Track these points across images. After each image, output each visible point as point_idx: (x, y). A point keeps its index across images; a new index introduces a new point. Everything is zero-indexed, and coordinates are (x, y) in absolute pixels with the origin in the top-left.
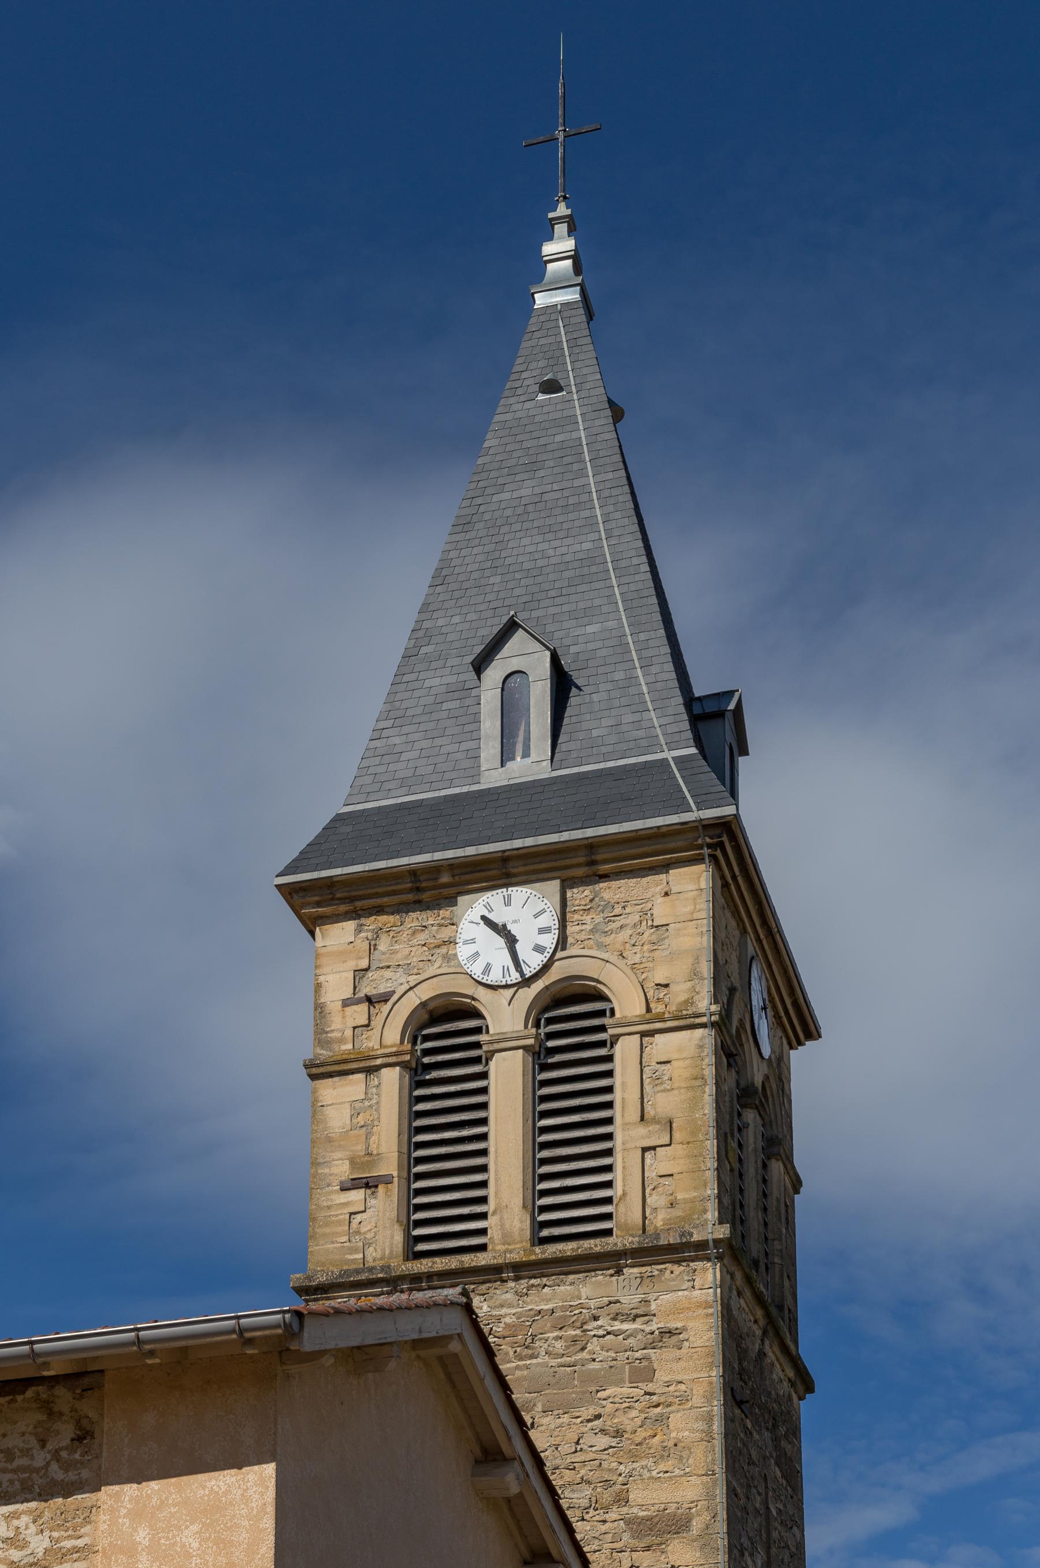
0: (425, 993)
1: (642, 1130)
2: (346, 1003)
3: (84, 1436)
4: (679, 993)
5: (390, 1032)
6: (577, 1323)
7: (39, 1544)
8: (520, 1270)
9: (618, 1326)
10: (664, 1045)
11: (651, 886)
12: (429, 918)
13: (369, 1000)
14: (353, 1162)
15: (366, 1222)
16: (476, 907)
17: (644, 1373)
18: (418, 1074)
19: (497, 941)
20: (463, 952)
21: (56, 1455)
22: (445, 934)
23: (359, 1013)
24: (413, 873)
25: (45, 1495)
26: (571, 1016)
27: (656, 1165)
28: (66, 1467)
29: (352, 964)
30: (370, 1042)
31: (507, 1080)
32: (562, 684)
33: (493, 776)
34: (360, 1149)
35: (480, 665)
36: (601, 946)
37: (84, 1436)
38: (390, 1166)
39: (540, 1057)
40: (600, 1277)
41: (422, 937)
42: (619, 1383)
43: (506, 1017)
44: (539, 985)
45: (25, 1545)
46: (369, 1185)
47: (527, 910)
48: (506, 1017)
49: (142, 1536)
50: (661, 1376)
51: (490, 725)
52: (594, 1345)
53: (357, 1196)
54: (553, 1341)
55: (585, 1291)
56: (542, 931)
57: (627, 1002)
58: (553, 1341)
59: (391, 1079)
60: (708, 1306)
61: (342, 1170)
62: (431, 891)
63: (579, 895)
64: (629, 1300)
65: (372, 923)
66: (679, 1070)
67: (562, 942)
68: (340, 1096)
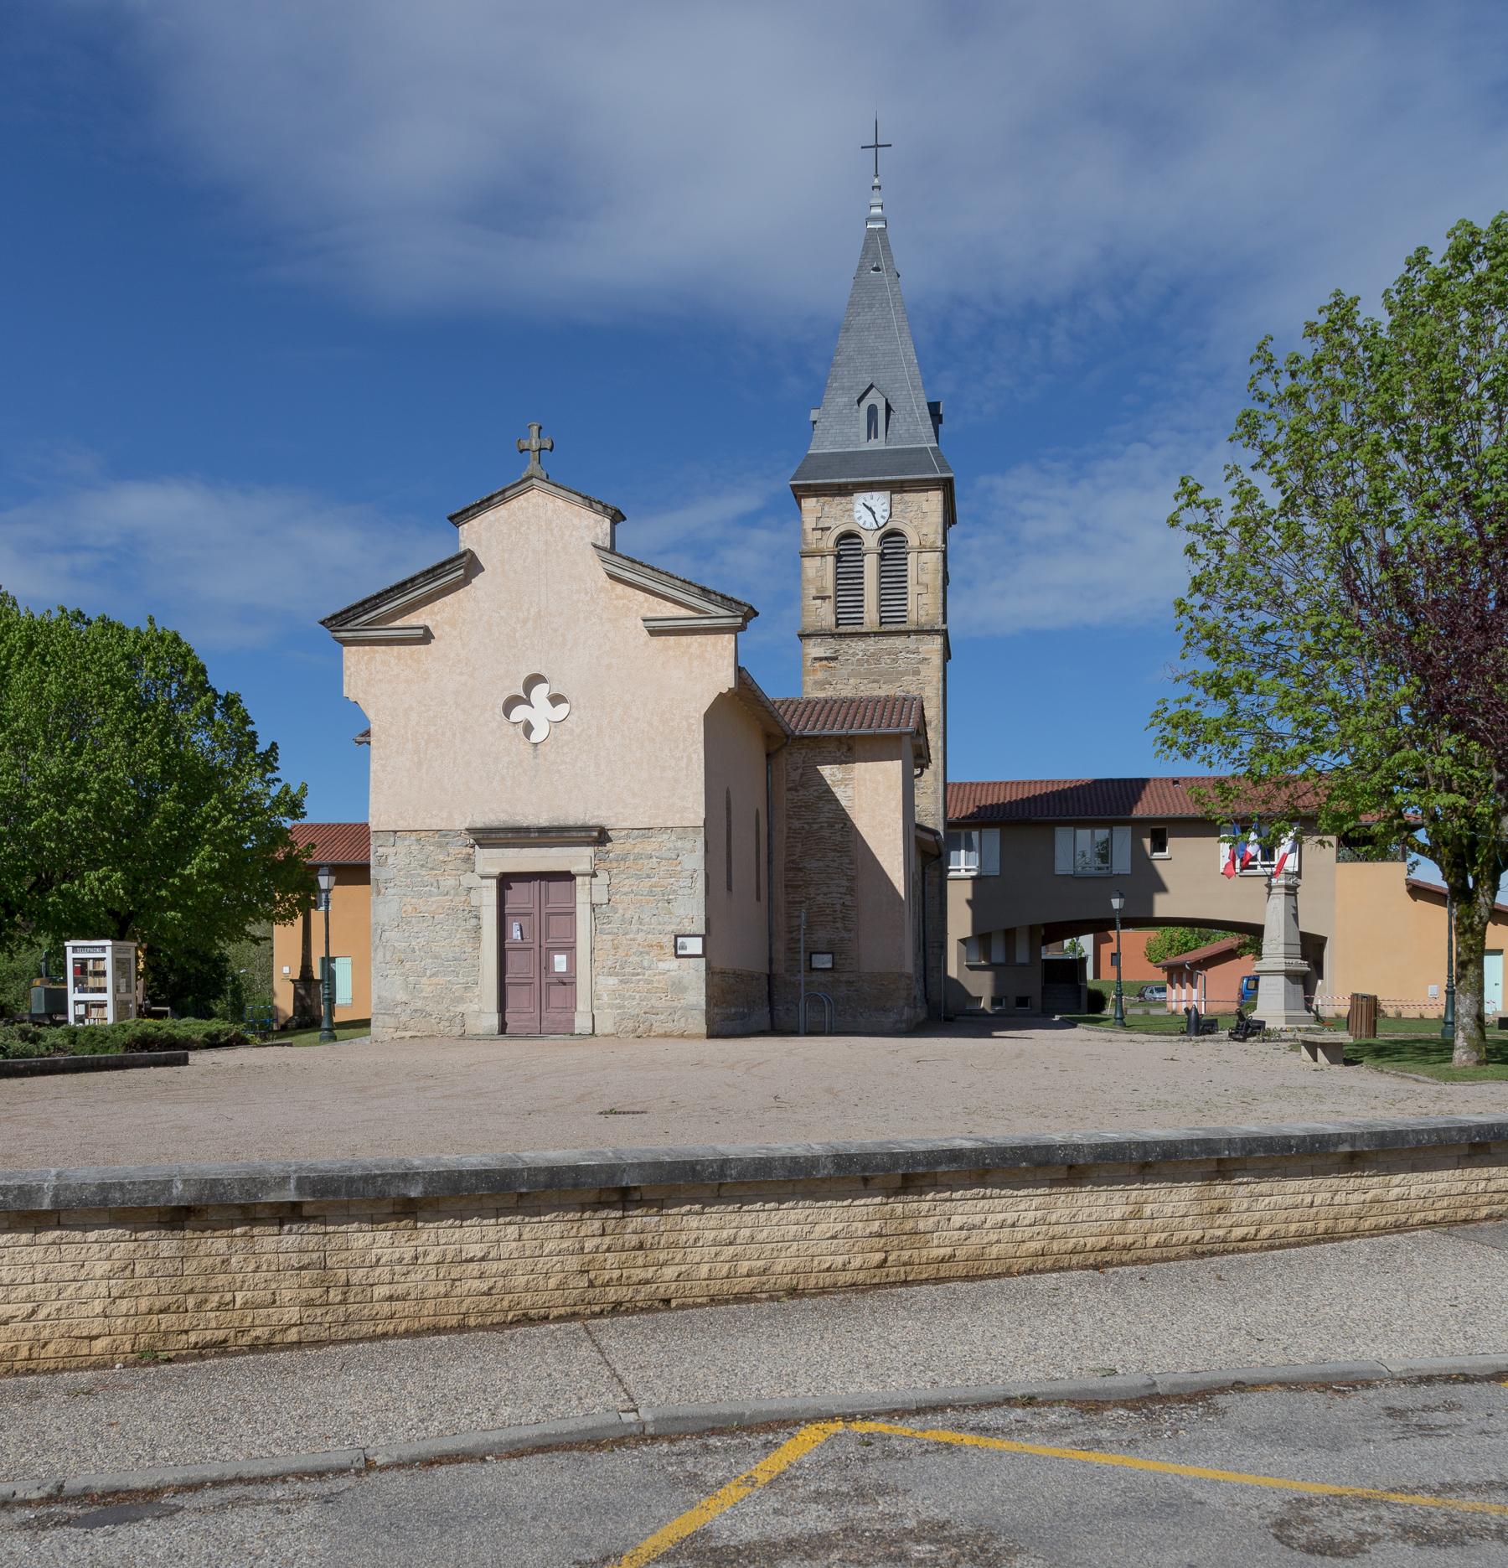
0: (842, 529)
3: (850, 749)
4: (931, 538)
5: (829, 542)
6: (894, 654)
7: (840, 776)
8: (876, 634)
10: (926, 557)
11: (922, 496)
12: (843, 500)
15: (822, 612)
16: (860, 498)
17: (917, 672)
18: (838, 558)
19: (868, 512)
20: (857, 515)
24: (839, 485)
25: (841, 763)
26: (892, 537)
27: (924, 599)
30: (822, 545)
31: (871, 564)
32: (888, 409)
33: (866, 447)
35: (859, 401)
37: (850, 749)
38: (830, 592)
39: (882, 556)
43: (871, 541)
46: (823, 598)
47: (879, 501)
48: (871, 541)
51: (864, 424)
54: (887, 659)
57: (913, 540)
58: (887, 659)
59: (830, 560)
61: (814, 593)
62: (845, 490)
63: (896, 497)
64: (912, 647)
65: (822, 499)
66: (930, 567)
68: (811, 565)
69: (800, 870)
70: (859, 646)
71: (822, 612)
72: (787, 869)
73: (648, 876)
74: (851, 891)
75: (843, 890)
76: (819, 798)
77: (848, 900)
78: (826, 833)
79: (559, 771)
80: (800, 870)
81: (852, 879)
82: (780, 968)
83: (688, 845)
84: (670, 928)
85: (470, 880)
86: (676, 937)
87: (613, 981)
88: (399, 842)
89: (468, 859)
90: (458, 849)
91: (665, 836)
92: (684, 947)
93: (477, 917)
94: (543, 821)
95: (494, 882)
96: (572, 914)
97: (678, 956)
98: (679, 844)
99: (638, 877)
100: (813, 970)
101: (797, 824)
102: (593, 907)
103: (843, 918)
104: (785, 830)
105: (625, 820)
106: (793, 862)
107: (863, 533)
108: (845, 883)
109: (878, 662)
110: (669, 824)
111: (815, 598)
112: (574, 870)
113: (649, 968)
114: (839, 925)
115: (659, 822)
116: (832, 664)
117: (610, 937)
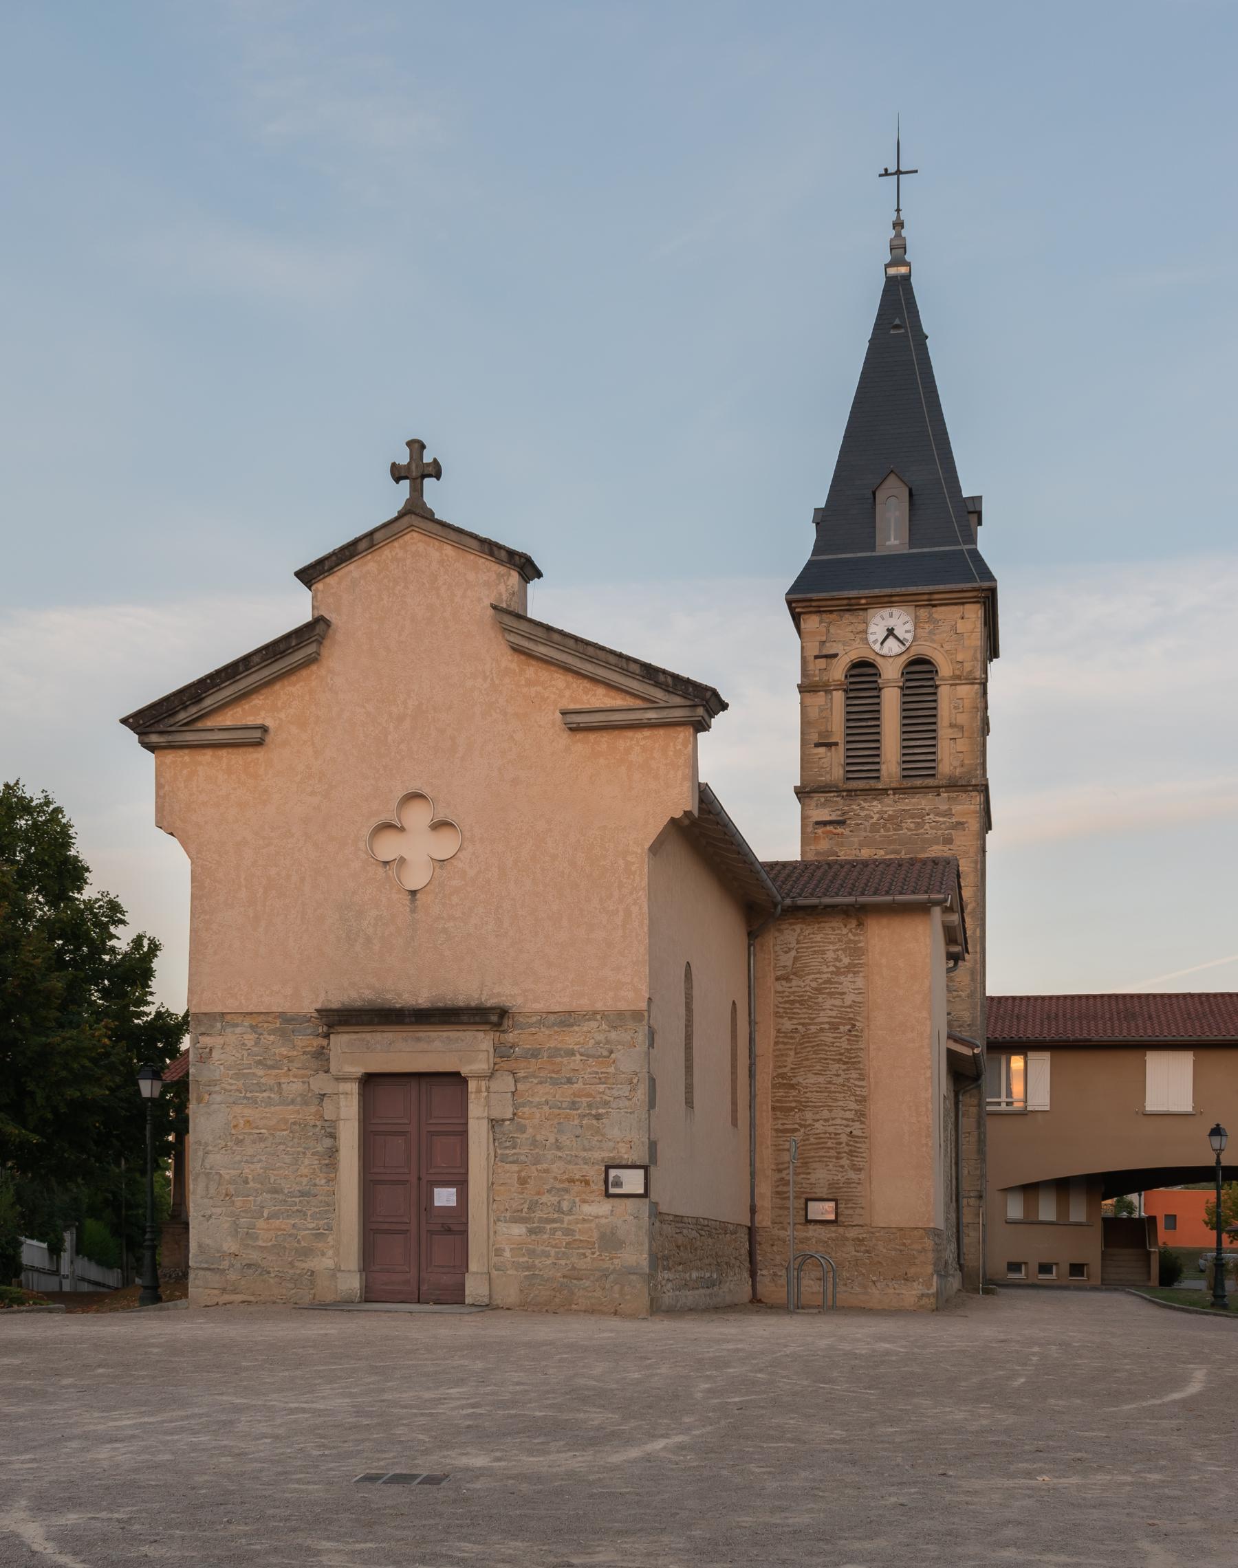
1: (950, 731)
2: (816, 657)
6: (920, 815)
7: (846, 961)
9: (938, 819)
13: (826, 656)
14: (820, 734)
17: (948, 841)
21: (850, 930)
22: (861, 627)
23: (822, 663)
28: (854, 935)
29: (819, 638)
34: (823, 728)
36: (933, 641)
40: (930, 796)
41: (850, 628)
42: (938, 844)
44: (904, 657)
45: (840, 961)
46: (829, 745)
49: (884, 961)
50: (957, 842)
52: (927, 826)
53: (822, 750)
55: (923, 802)
56: (907, 631)
60: (976, 812)
64: (944, 807)
67: (915, 639)
69: (792, 1087)
70: (874, 809)
71: (825, 762)
72: (774, 1086)
73: (569, 1081)
74: (861, 1116)
75: (849, 1115)
76: (819, 990)
77: (856, 1128)
78: (828, 1037)
80: (792, 1087)
81: (862, 1100)
82: (764, 1219)
83: (626, 1037)
84: (597, 1155)
85: (320, 1083)
86: (608, 1168)
88: (229, 1030)
89: (321, 1055)
90: (307, 1041)
91: (594, 1024)
92: (618, 1184)
95: (354, 1088)
96: (463, 1134)
97: (608, 1195)
98: (613, 1035)
99: (555, 1083)
100: (808, 1222)
101: (788, 1025)
102: (494, 1123)
103: (850, 1153)
104: (773, 1033)
106: (782, 1076)
107: (880, 662)
108: (853, 1106)
109: (899, 827)
110: (599, 1006)
111: (818, 745)
112: (464, 1071)
113: (570, 1212)
114: (845, 1162)
115: (584, 1004)
116: (840, 830)
117: (515, 1167)
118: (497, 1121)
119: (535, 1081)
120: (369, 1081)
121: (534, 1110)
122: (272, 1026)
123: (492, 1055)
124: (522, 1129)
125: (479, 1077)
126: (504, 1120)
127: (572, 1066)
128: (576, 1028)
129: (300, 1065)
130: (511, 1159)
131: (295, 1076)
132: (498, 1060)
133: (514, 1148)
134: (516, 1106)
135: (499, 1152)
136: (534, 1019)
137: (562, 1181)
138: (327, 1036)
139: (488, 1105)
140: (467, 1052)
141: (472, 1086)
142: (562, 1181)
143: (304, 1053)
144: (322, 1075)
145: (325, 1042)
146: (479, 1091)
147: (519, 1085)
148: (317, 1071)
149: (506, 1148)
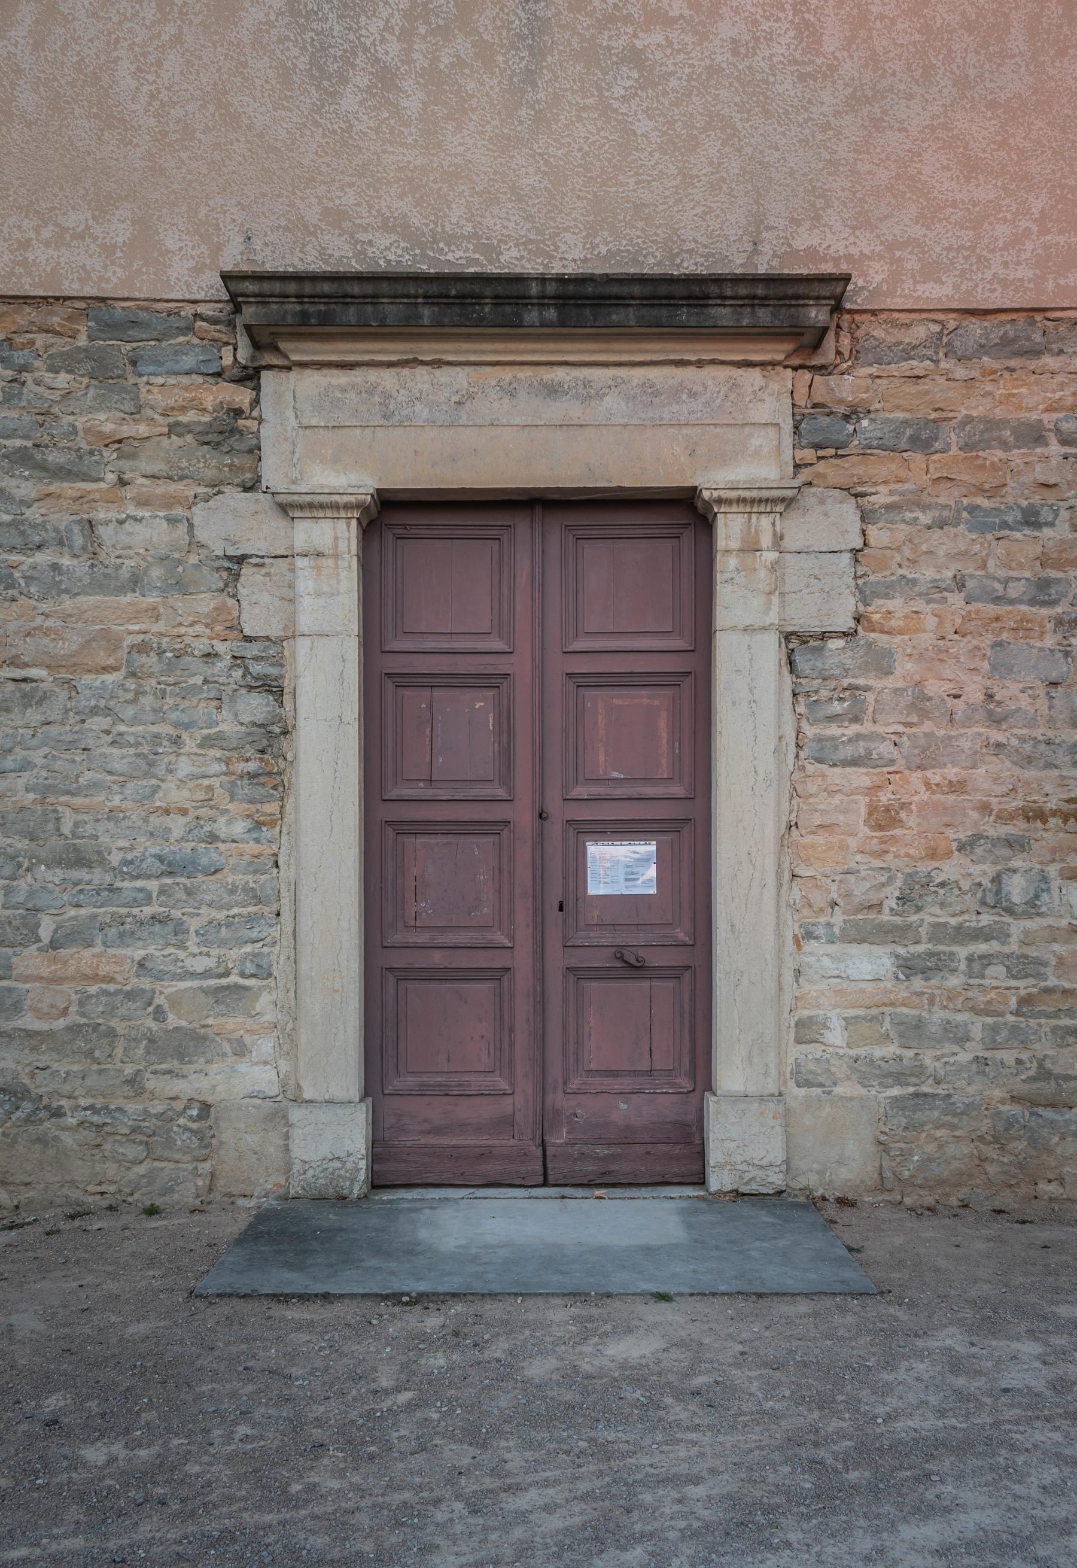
79: (635, 57)
85: (231, 521)
87: (870, 964)
90: (181, 390)
93: (273, 688)
94: (572, 255)
95: (341, 536)
96: (690, 684)
102: (797, 644)
105: (931, 271)
112: (712, 480)
117: (860, 777)
118: (803, 638)
119: (925, 519)
120: (392, 517)
121: (919, 605)
122: (61, 345)
123: (788, 440)
124: (881, 663)
125: (757, 502)
126: (824, 636)
127: (1040, 473)
128: (1050, 361)
129: (159, 467)
130: (847, 752)
131: (143, 502)
132: (809, 454)
133: (856, 719)
134: (864, 595)
135: (810, 731)
136: (920, 332)
137: (1005, 817)
138: (249, 376)
139: (777, 589)
140: (706, 422)
141: (729, 529)
142: (1005, 817)
143: (174, 429)
144: (233, 497)
145: (242, 397)
146: (751, 548)
147: (873, 531)
148: (216, 486)
149: (832, 718)
